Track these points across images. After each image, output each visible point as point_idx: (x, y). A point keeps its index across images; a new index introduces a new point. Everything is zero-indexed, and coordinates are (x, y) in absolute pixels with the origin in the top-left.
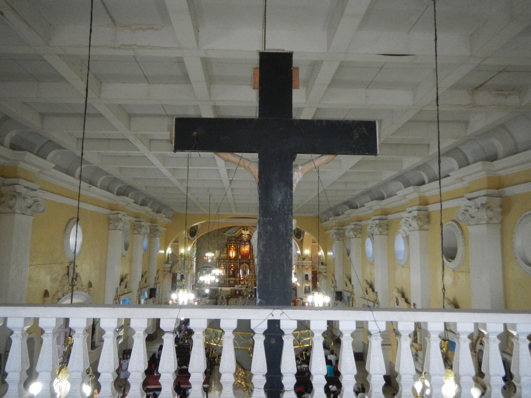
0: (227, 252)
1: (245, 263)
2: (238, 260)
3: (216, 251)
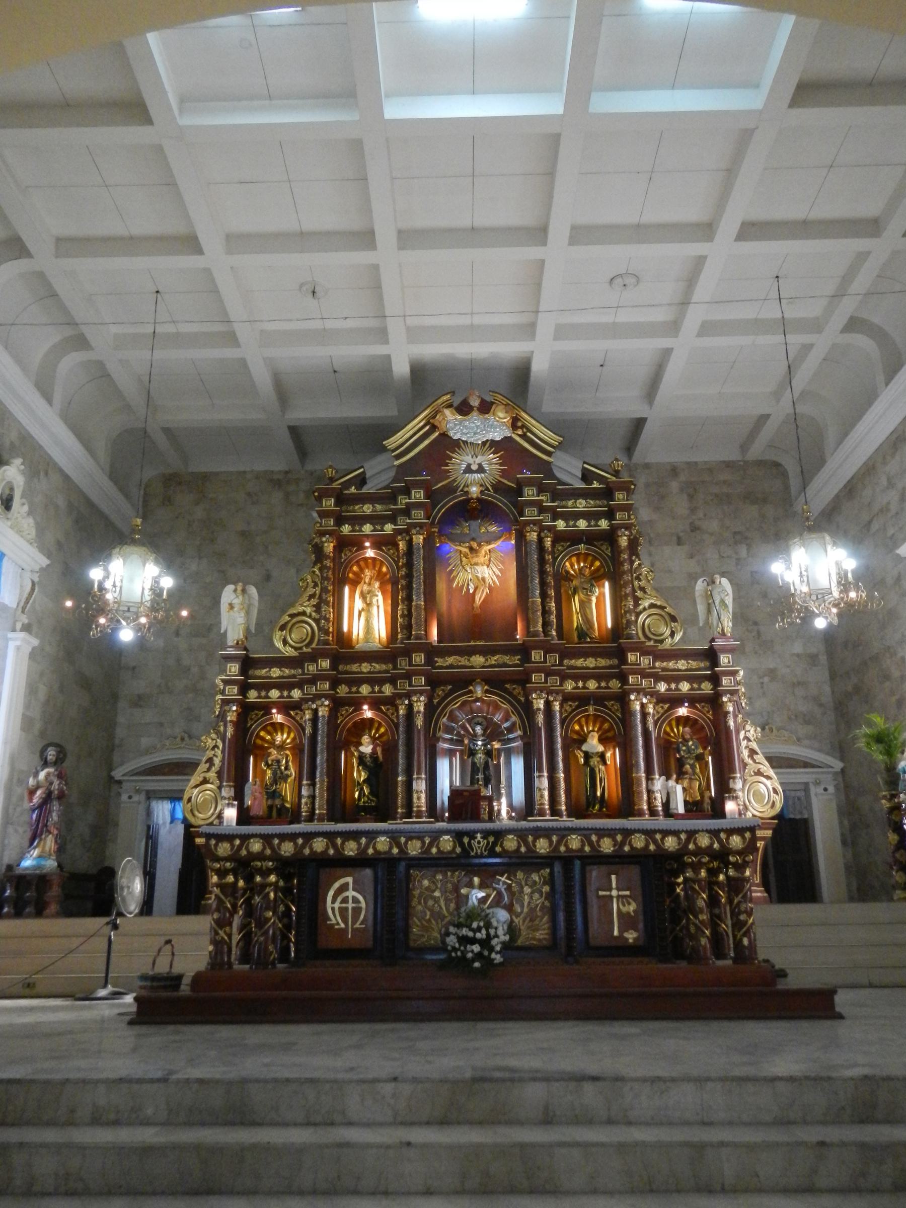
0: (318, 608)
1: (479, 691)
2: (419, 648)
3: (228, 595)
